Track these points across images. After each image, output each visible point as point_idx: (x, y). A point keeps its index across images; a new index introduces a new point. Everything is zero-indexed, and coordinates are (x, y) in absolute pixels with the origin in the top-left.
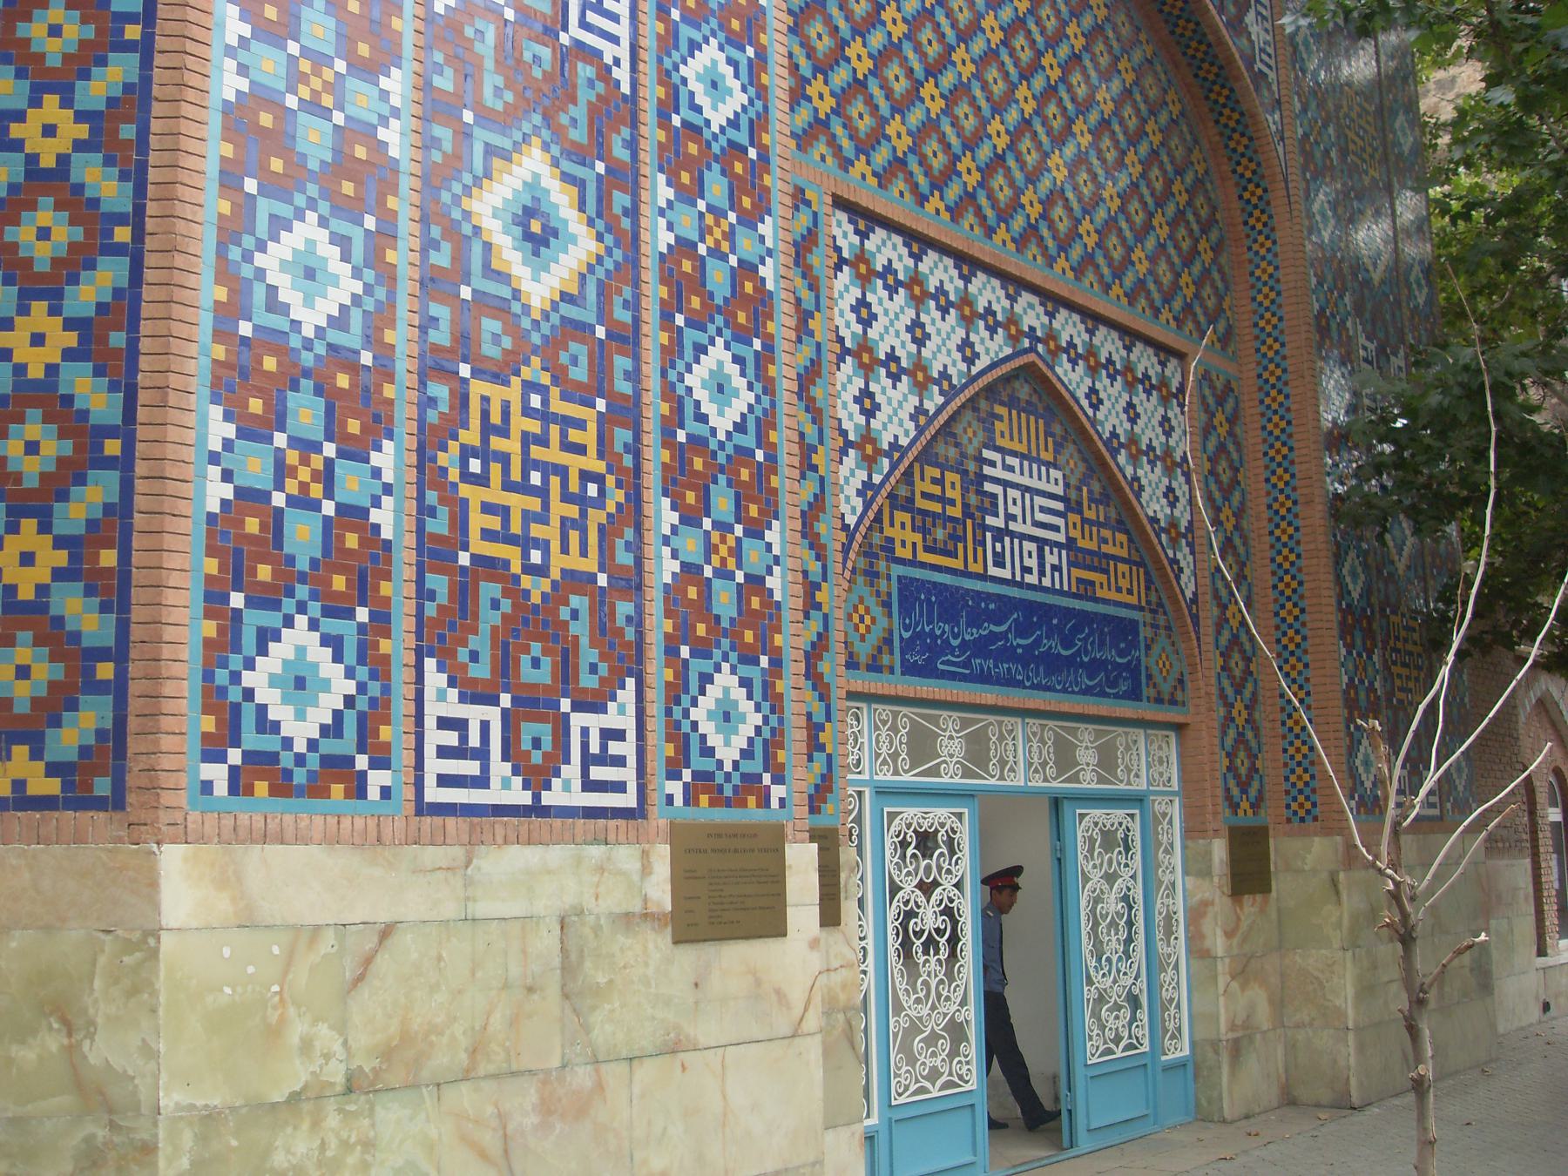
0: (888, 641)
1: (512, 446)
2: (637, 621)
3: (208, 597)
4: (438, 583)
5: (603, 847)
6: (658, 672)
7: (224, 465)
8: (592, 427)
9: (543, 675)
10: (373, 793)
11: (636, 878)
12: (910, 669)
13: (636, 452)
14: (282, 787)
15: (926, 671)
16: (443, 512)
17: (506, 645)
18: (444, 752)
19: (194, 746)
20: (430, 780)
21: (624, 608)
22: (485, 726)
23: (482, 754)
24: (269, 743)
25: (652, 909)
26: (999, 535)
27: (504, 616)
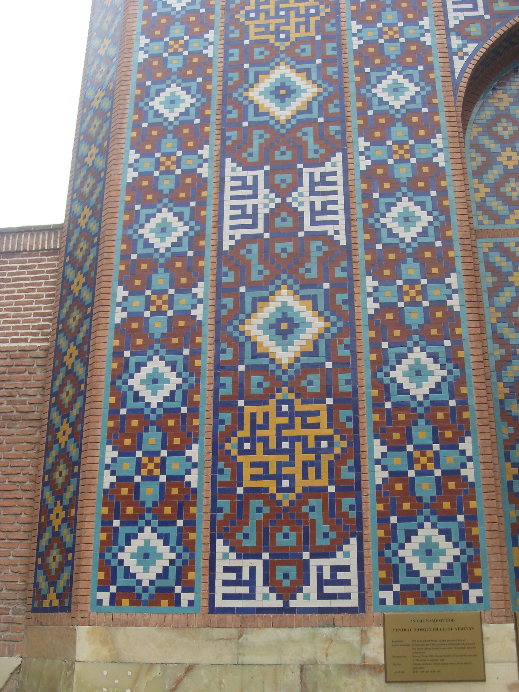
1: (271, 433)
2: (358, 507)
3: (103, 523)
4: (225, 504)
5: (331, 629)
7: (112, 468)
8: (324, 413)
9: (292, 541)
10: (184, 603)
11: (356, 645)
13: (356, 421)
14: (136, 601)
16: (228, 471)
17: (266, 529)
18: (226, 583)
19: (94, 585)
20: (218, 597)
22: (253, 570)
23: (251, 583)
24: (130, 583)
25: (368, 662)
27: (265, 515)
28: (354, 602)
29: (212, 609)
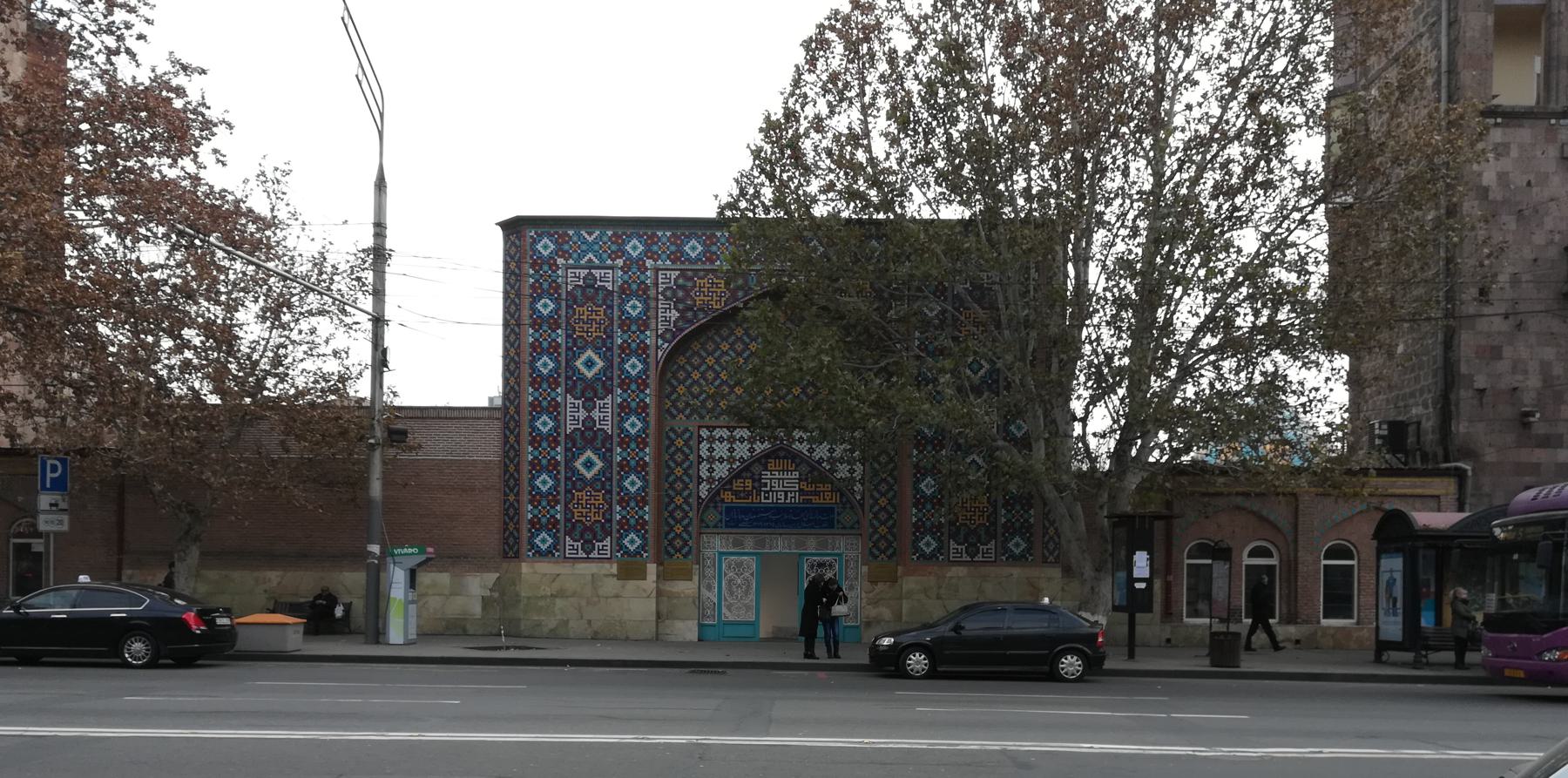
0: (721, 521)
4: (569, 525)
6: (615, 535)
12: (727, 526)
13: (611, 499)
15: (736, 526)
21: (608, 525)
26: (767, 492)
28: (609, 556)
29: (565, 557)
